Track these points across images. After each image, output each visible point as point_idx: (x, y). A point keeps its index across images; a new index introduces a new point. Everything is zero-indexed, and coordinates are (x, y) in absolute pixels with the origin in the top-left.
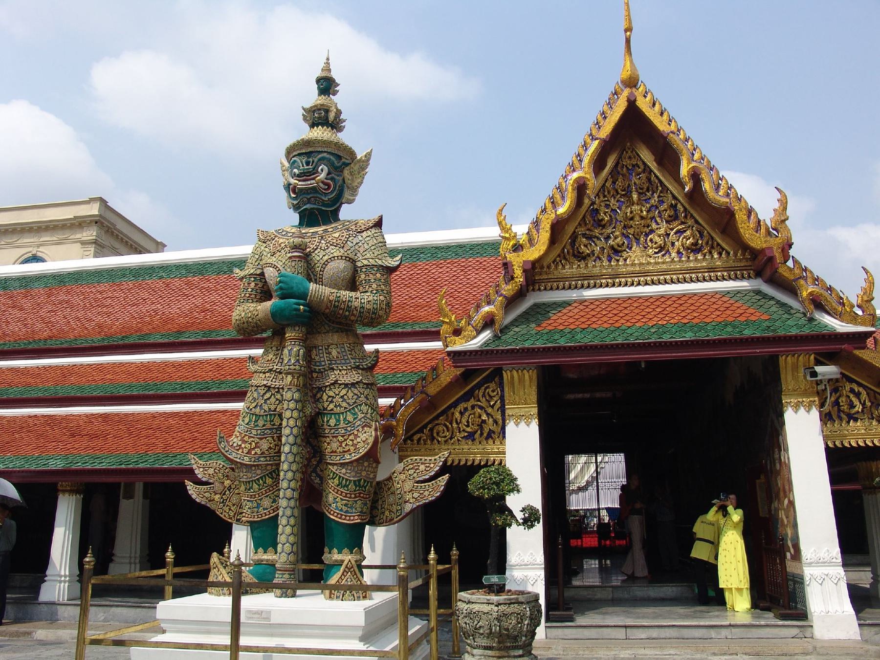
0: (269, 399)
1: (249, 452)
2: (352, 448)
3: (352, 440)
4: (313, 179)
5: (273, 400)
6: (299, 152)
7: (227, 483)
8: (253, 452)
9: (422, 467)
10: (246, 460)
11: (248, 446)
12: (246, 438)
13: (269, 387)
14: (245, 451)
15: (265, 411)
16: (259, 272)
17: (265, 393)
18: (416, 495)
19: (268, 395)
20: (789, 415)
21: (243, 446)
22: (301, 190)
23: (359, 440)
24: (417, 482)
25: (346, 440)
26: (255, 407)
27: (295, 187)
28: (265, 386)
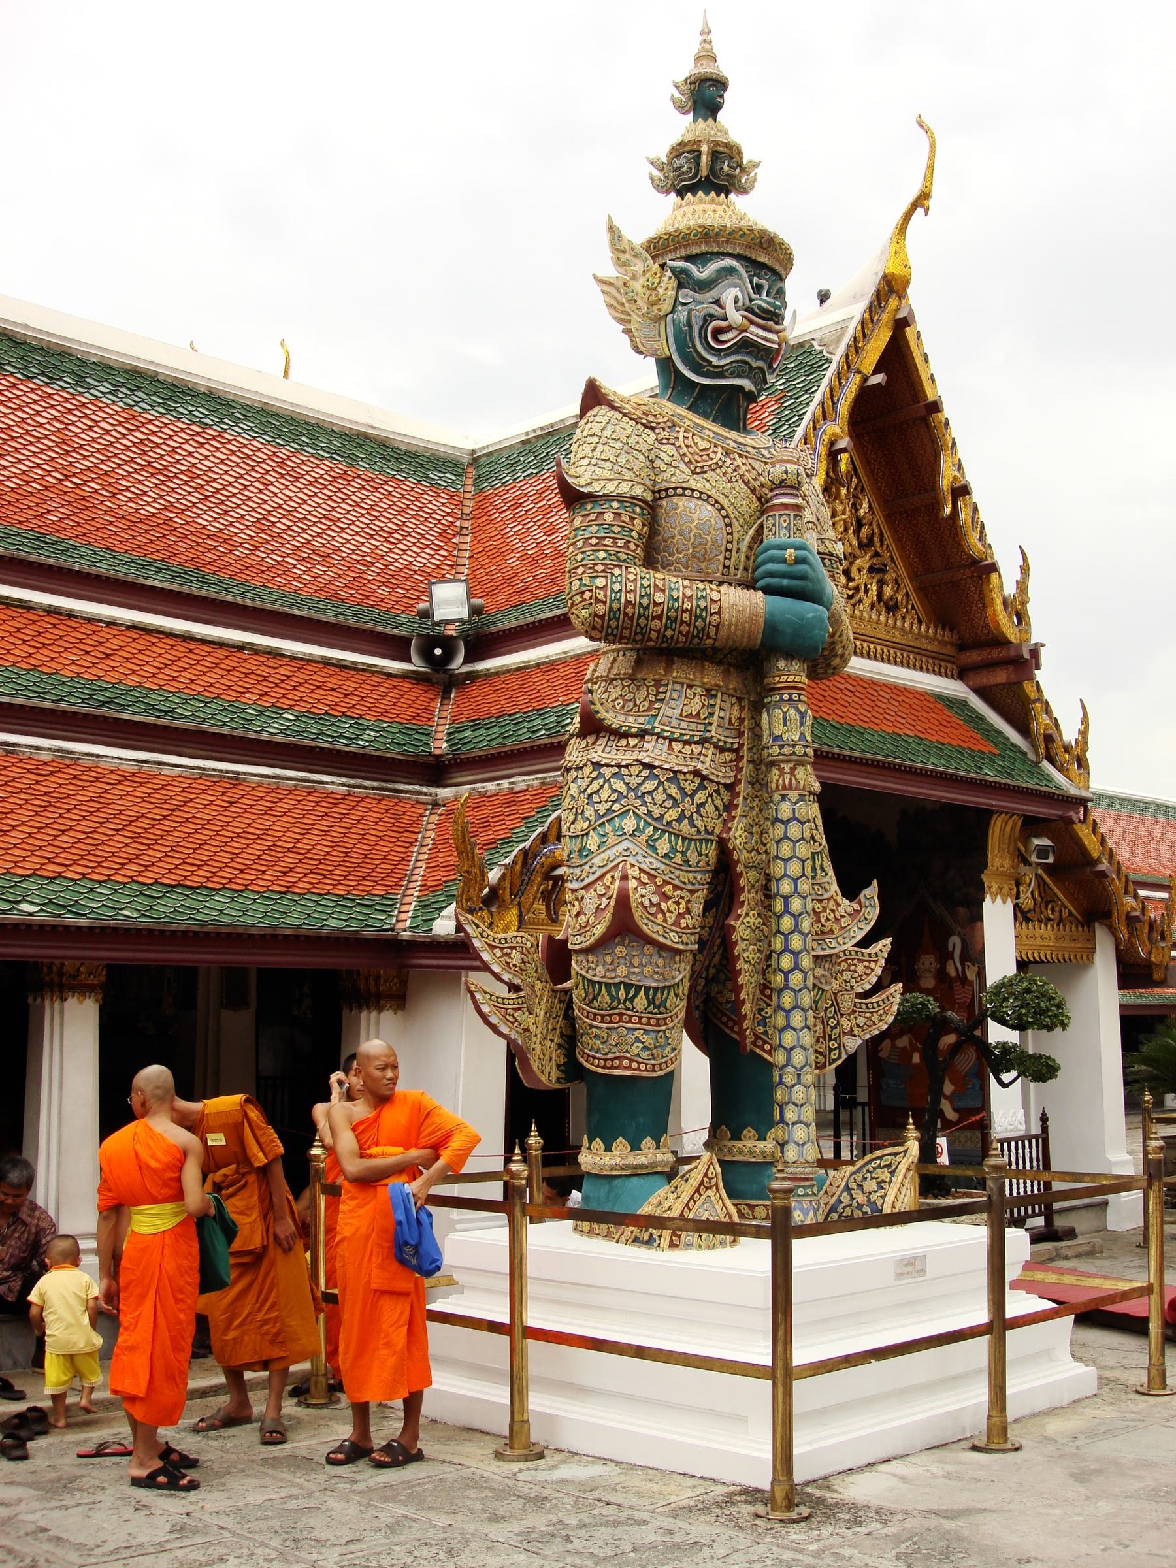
0: (702, 804)
1: (676, 923)
2: (835, 927)
3: (833, 911)
4: (777, 332)
5: (709, 807)
6: (739, 250)
7: (538, 985)
8: (683, 923)
9: (860, 967)
10: (672, 940)
11: (673, 907)
12: (667, 889)
13: (704, 778)
14: (671, 918)
15: (699, 832)
16: (649, 497)
17: (695, 792)
18: (861, 1021)
19: (701, 797)
20: (987, 905)
21: (663, 906)
22: (746, 345)
23: (841, 910)
24: (859, 996)
25: (825, 909)
26: (679, 820)
27: (729, 328)
28: (697, 773)
